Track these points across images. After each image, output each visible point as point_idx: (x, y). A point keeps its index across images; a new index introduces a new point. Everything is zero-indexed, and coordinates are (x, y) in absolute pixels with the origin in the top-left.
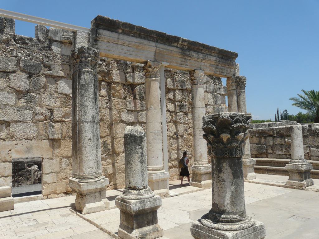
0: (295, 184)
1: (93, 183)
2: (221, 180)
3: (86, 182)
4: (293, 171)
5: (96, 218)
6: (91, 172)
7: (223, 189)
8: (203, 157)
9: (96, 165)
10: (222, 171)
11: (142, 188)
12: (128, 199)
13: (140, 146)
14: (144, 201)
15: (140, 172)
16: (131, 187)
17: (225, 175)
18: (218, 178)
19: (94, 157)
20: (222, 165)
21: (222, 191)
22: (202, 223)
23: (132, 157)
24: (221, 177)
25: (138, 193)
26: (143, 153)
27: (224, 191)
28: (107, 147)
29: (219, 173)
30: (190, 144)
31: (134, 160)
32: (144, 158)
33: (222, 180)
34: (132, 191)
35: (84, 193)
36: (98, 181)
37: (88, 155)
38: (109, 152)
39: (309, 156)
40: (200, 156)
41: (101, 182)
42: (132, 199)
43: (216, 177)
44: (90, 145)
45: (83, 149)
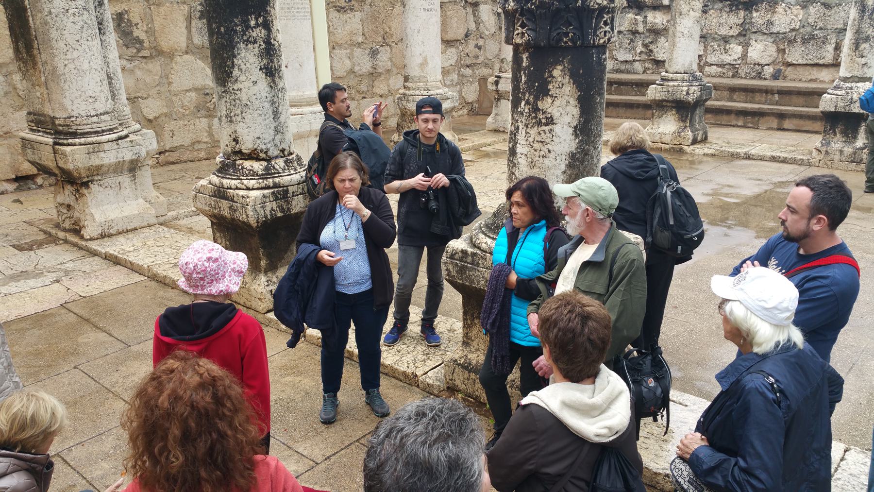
0: (663, 140)
1: (106, 146)
2: (544, 121)
3: (81, 145)
4: (664, 103)
5: (132, 249)
6: (93, 113)
7: (549, 146)
8: (430, 66)
9: (106, 88)
10: (549, 90)
11: (276, 153)
12: (237, 188)
13: (261, 20)
14: (287, 191)
15: (267, 105)
16: (240, 152)
17: (557, 103)
18: (533, 115)
19: (98, 62)
20: (550, 72)
21: (542, 153)
22: (474, 245)
23: (235, 56)
24: (544, 112)
25: (266, 169)
26: (272, 41)
27: (549, 151)
28: (132, 32)
29: (537, 99)
30: (388, 30)
31: (243, 67)
32: (275, 61)
33: (547, 118)
34: (247, 164)
35: (80, 178)
36: (121, 138)
37: (76, 54)
38: (139, 51)
39: (702, 64)
40: (421, 64)
41: (131, 142)
42: (248, 189)
43: (526, 110)
44: (77, 19)
45: (54, 34)
